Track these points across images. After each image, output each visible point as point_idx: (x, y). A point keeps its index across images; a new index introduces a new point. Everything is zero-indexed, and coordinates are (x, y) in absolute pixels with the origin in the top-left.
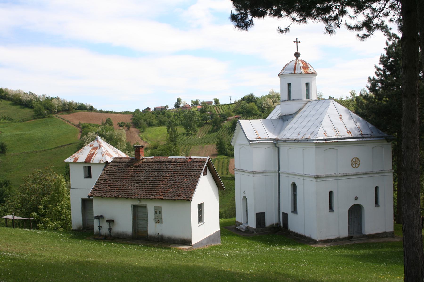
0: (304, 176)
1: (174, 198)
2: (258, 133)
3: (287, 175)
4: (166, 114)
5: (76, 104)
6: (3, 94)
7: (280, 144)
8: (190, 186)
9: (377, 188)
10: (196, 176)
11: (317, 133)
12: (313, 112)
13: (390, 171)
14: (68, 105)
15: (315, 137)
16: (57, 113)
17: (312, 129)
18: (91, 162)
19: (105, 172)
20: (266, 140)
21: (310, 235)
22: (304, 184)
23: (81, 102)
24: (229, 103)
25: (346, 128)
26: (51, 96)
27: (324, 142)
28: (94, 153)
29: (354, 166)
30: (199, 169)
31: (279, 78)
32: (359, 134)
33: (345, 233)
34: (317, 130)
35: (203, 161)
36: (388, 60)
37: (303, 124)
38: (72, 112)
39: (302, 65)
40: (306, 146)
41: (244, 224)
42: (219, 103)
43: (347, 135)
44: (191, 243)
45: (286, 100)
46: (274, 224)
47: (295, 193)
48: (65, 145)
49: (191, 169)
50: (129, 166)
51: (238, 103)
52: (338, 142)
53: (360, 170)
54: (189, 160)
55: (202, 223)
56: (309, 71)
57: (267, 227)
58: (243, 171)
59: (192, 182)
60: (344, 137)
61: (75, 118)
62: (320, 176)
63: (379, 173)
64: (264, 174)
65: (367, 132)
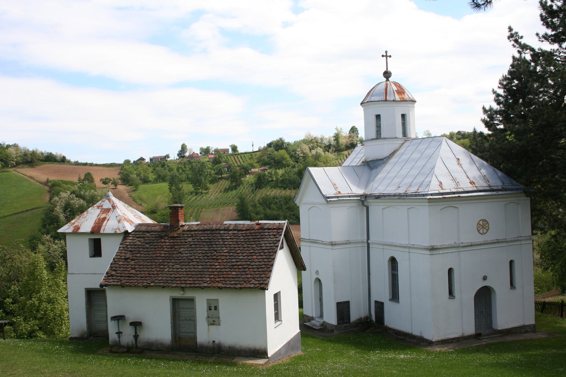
0: (409, 248)
1: (239, 286)
2: (337, 186)
3: (381, 247)
4: (166, 166)
5: (42, 153)
7: (370, 201)
8: (263, 266)
10: (271, 251)
11: (428, 185)
12: (416, 156)
13: (528, 238)
14: (31, 155)
15: (426, 190)
16: (14, 166)
17: (420, 179)
18: (102, 231)
19: (124, 247)
20: (349, 197)
21: (421, 332)
22: (409, 259)
23: (49, 151)
24: (251, 151)
25: (468, 177)
26: (7, 143)
27: (441, 197)
28: (104, 219)
30: (275, 239)
31: (361, 109)
32: (486, 185)
33: (470, 329)
34: (428, 179)
35: (280, 228)
36: (511, 83)
37: (404, 172)
38: (37, 165)
39: (395, 88)
41: (317, 319)
42: (237, 151)
43: (470, 187)
44: (267, 355)
45: (373, 139)
46: (361, 318)
47: (394, 272)
48: (27, 211)
49: (261, 240)
50: (162, 237)
51: (263, 151)
52: (459, 197)
53: (488, 237)
54: (257, 227)
55: (278, 323)
56: (406, 97)
58: (315, 242)
59: (266, 260)
60: (466, 190)
61: (40, 174)
62: (435, 247)
64: (348, 246)
65: (496, 182)
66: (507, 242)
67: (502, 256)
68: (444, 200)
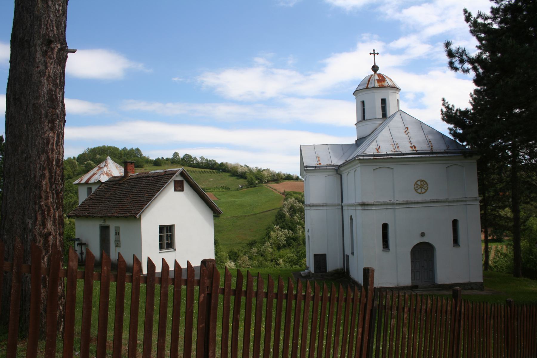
6: (224, 167)
9: (455, 223)
16: (266, 183)
20: (326, 167)
23: (288, 173)
26: (263, 168)
29: (419, 191)
40: (354, 167)
43: (409, 150)
46: (338, 269)
56: (385, 84)
61: (281, 187)
62: (367, 203)
63: (458, 201)
64: (325, 208)
67: (446, 215)
68: (376, 161)
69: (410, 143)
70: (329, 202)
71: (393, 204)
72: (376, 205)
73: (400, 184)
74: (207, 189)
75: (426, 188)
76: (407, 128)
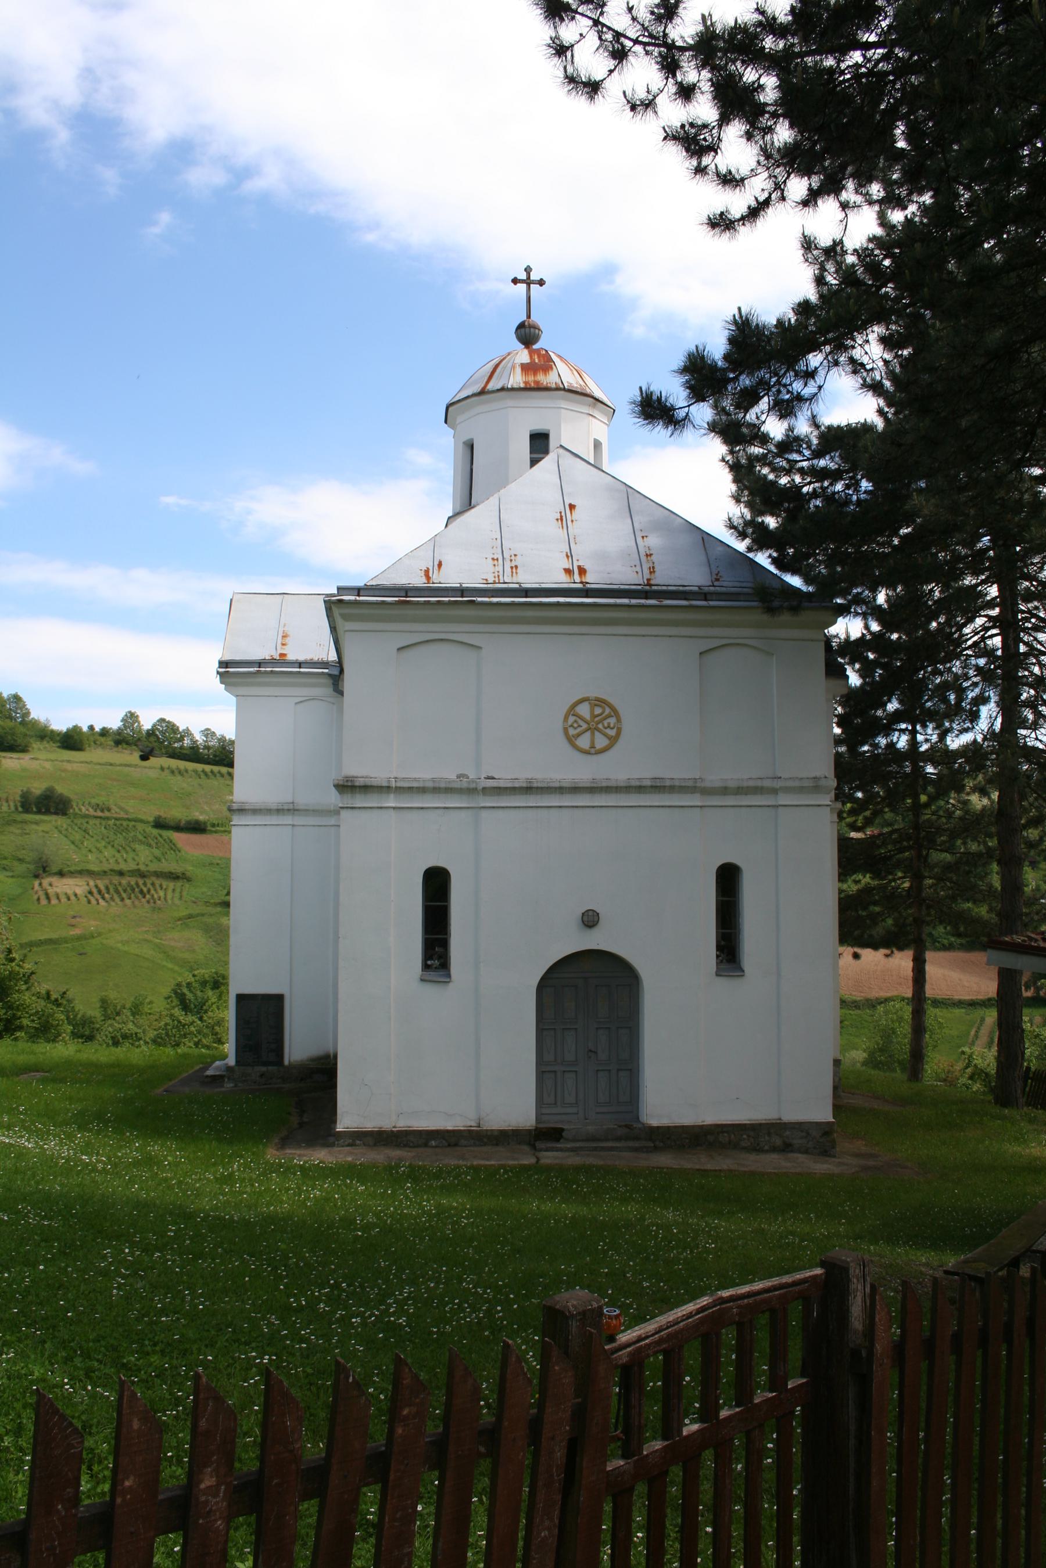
9: (728, 879)
29: (584, 742)
56: (550, 379)
57: (291, 1066)
62: (359, 782)
64: (288, 820)
66: (706, 792)
68: (409, 612)
69: (569, 556)
70: (303, 800)
71: (471, 791)
72: (400, 790)
73: (510, 709)
74: (213, 825)
75: (612, 733)
76: (572, 507)
